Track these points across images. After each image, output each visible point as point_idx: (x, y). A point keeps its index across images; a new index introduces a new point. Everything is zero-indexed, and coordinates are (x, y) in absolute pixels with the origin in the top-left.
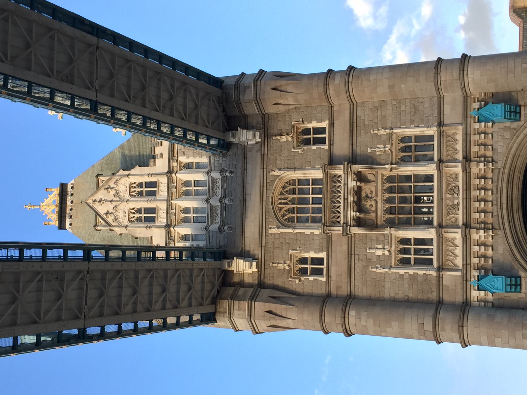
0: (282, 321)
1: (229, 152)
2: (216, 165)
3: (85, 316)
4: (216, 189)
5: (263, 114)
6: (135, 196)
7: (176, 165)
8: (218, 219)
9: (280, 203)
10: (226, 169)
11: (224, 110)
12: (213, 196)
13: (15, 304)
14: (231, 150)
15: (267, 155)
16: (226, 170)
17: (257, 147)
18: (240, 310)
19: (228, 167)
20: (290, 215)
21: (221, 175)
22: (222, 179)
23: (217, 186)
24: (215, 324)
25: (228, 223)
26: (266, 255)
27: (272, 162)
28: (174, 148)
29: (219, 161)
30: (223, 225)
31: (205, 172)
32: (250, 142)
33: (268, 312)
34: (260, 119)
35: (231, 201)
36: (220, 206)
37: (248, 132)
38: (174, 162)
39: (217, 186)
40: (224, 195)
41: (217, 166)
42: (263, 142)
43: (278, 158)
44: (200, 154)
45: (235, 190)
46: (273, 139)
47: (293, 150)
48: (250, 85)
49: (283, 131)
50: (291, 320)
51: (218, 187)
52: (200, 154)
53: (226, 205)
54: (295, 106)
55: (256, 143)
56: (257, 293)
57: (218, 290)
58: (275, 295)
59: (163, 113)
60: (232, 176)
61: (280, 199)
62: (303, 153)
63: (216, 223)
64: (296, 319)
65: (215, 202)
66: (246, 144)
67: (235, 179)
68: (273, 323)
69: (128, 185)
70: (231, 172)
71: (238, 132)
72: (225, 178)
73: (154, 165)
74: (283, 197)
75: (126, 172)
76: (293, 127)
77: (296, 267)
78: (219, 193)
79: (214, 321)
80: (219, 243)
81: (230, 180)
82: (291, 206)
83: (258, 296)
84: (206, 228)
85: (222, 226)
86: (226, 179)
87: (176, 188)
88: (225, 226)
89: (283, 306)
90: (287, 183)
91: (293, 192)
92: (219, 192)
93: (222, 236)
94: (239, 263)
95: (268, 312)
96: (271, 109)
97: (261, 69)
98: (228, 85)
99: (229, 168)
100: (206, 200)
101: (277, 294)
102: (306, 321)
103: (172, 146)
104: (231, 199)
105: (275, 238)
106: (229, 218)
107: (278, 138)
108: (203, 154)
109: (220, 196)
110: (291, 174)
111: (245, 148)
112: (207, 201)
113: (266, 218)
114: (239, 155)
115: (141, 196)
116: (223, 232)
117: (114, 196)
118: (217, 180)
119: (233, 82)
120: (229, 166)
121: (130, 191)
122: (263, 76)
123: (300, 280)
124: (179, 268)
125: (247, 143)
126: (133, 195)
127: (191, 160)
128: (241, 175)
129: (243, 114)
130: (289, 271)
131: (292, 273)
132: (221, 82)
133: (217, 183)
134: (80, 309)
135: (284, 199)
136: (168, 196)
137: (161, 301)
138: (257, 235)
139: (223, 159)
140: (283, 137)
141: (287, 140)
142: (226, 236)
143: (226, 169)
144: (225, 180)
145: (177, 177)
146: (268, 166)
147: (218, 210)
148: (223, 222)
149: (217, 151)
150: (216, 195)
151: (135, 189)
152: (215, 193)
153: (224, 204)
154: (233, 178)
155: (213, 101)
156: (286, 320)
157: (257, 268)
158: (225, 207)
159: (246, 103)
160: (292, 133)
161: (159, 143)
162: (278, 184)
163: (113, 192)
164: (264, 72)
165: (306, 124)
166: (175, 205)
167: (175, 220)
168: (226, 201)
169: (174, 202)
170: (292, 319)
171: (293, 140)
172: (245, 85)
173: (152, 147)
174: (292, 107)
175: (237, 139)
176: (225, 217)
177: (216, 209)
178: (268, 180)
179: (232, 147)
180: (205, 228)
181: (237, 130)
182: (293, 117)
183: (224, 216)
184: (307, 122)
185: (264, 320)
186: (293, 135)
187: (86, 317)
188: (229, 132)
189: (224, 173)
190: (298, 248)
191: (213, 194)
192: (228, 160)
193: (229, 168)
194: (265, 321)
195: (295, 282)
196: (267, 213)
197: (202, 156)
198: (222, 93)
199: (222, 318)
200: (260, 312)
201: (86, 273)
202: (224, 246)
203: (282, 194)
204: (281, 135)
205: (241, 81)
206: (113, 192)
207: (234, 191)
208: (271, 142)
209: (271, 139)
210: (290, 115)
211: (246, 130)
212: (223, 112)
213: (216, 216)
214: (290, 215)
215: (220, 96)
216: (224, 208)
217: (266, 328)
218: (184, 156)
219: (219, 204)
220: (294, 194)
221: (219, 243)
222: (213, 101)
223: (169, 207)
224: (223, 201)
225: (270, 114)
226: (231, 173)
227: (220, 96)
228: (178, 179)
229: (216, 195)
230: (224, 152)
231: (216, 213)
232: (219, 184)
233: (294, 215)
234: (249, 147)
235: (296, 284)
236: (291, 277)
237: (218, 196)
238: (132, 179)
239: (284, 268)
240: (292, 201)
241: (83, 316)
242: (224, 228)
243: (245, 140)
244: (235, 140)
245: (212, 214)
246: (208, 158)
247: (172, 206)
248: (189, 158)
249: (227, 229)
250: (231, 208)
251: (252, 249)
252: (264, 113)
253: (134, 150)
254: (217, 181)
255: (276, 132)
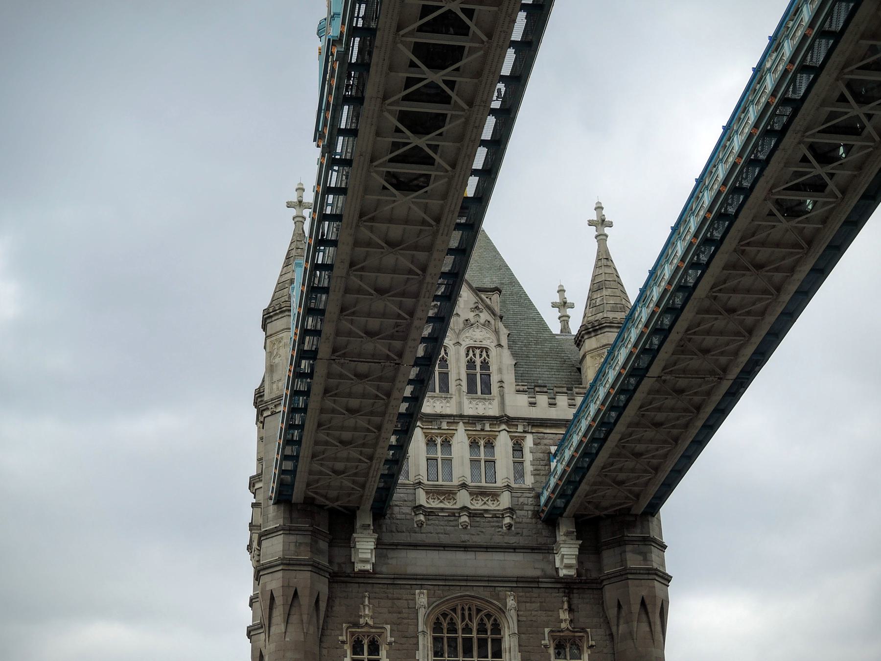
0: (282, 616)
1: (540, 522)
2: (521, 500)
3: (334, 360)
4: (482, 500)
5: (602, 581)
6: (467, 357)
7: (518, 431)
8: (435, 504)
9: (463, 609)
10: (514, 517)
11: (608, 516)
12: (471, 494)
13: (375, 293)
14: (545, 526)
15: (538, 587)
16: (512, 518)
17: (550, 571)
18: (296, 545)
19: (518, 520)
20: (445, 625)
21: (506, 509)
22: (498, 510)
23: (488, 501)
24: (272, 502)
25: (429, 520)
26: (380, 586)
27: (528, 594)
28: (547, 426)
29: (527, 505)
30: (425, 511)
31: (509, 481)
32: (558, 559)
33: (296, 593)
34: (594, 575)
35: (464, 526)
36: (455, 507)
37: (574, 557)
38: (524, 428)
39: (488, 501)
40: (473, 514)
41: (518, 501)
42: (558, 580)
43: (536, 606)
44: (538, 472)
45: (482, 532)
46: (563, 597)
47: (547, 630)
48: (649, 562)
49: (576, 613)
50: (283, 631)
51: (485, 503)
52: (538, 472)
53: (457, 518)
54: (615, 633)
55: (556, 568)
56: (322, 572)
57: (326, 506)
58: (320, 602)
59: (616, 446)
60: (504, 526)
61: (470, 609)
62: (543, 647)
63: (428, 499)
64: (287, 639)
65: (463, 499)
66: (555, 552)
67: (500, 534)
68: (279, 601)
69: (485, 343)
70: (510, 526)
71: (574, 542)
72: (501, 516)
73: (518, 391)
74: (474, 612)
75: (504, 342)
76: (583, 630)
77: (364, 636)
78: (475, 505)
79: (276, 500)
80: (397, 506)
81: (497, 524)
82: (460, 626)
83: (318, 575)
84: (420, 483)
85: (424, 511)
86: (499, 517)
87: (482, 430)
88: (424, 515)
89: (305, 617)
90: (495, 620)
91: (482, 629)
92: (478, 505)
93: (407, 510)
94: (368, 542)
95: (296, 593)
96: (611, 593)
97: (671, 577)
98: (649, 526)
99: (516, 523)
100: (466, 484)
101: (323, 605)
102: (284, 656)
103: (548, 424)
104: (467, 526)
105: (409, 601)
106: (437, 522)
107: (566, 606)
108: (537, 477)
109: (472, 507)
110: (509, 628)
111: (547, 549)
112: (464, 486)
113: (439, 585)
114: (537, 539)
115: (468, 367)
116: (415, 512)
117: (467, 320)
118: (496, 501)
119: (654, 534)
120: (520, 523)
121: (475, 347)
122: (662, 583)
123: (343, 642)
124: (374, 461)
125: (557, 554)
126: (468, 351)
127: (528, 457)
128: (506, 543)
129: (603, 548)
130: (356, 625)
131: (354, 630)
132: (653, 513)
133: (491, 501)
134: (344, 355)
135: (470, 615)
136: (469, 416)
137: (327, 440)
138: (411, 570)
139: (529, 512)
140: (567, 613)
141: (561, 621)
142: (408, 517)
143: (514, 517)
144: (498, 516)
145: (499, 431)
146: (521, 589)
147: (449, 502)
148: (430, 513)
149: (546, 505)
150: (472, 500)
151: (478, 356)
152: (476, 497)
153: (460, 514)
154: (500, 529)
155: (624, 503)
156: (284, 622)
157: (360, 571)
158: (455, 516)
159: (621, 554)
160: (573, 628)
161: (554, 400)
162: (492, 606)
163: (471, 316)
164: (666, 582)
165: (587, 651)
166: (454, 428)
167: (431, 429)
168: (464, 519)
169: (461, 427)
170: (285, 632)
171: (562, 631)
172: (648, 555)
173: (546, 387)
174: (614, 629)
175: (563, 538)
176: (439, 516)
177: (451, 499)
178: (499, 589)
179: (550, 528)
180: (420, 482)
181: (578, 539)
182: (598, 630)
183: (440, 514)
184: (590, 653)
185: (283, 586)
186: (570, 631)
187: (332, 361)
188: (574, 528)
189: (508, 515)
190: (393, 639)
191: (475, 494)
192: (528, 521)
193: (516, 523)
194: (281, 588)
195: (342, 635)
196: (447, 588)
197: (534, 475)
198: (636, 515)
199: (282, 514)
200: (296, 580)
201: (397, 362)
202: (392, 514)
203: (479, 611)
204: (571, 610)
205: (655, 547)
206: (471, 316)
207: (480, 531)
208: (557, 594)
209: (564, 594)
210: (601, 626)
211: (577, 553)
212: (604, 515)
213: (439, 499)
214: (445, 625)
215: (633, 512)
216: (454, 514)
217: (269, 588)
218: (534, 444)
219: (457, 506)
220: (479, 632)
221: (397, 506)
222: (624, 503)
223: (453, 418)
224: (465, 513)
225: (602, 592)
226: (509, 526)
227: (633, 512)
228: (497, 433)
229: (472, 500)
230: (543, 515)
231: (444, 499)
232: (491, 506)
233: (445, 631)
234: (551, 558)
235: (338, 635)
236: (348, 628)
237: (471, 504)
238: (493, 352)
239: (361, 615)
240: (467, 629)
241: (335, 358)
242: (421, 515)
243: (562, 553)
244: (561, 537)
245: (443, 493)
246: (531, 487)
247: (454, 423)
248: (531, 452)
249: (420, 520)
250: (453, 526)
251: (390, 561)
252: (604, 584)
253: (538, 346)
254: (494, 501)
255: (575, 601)
